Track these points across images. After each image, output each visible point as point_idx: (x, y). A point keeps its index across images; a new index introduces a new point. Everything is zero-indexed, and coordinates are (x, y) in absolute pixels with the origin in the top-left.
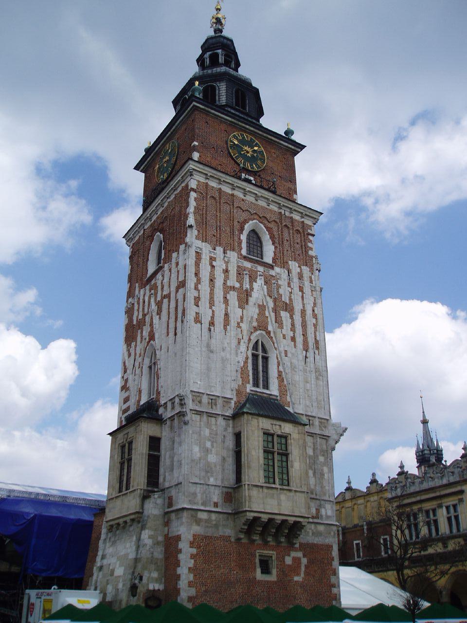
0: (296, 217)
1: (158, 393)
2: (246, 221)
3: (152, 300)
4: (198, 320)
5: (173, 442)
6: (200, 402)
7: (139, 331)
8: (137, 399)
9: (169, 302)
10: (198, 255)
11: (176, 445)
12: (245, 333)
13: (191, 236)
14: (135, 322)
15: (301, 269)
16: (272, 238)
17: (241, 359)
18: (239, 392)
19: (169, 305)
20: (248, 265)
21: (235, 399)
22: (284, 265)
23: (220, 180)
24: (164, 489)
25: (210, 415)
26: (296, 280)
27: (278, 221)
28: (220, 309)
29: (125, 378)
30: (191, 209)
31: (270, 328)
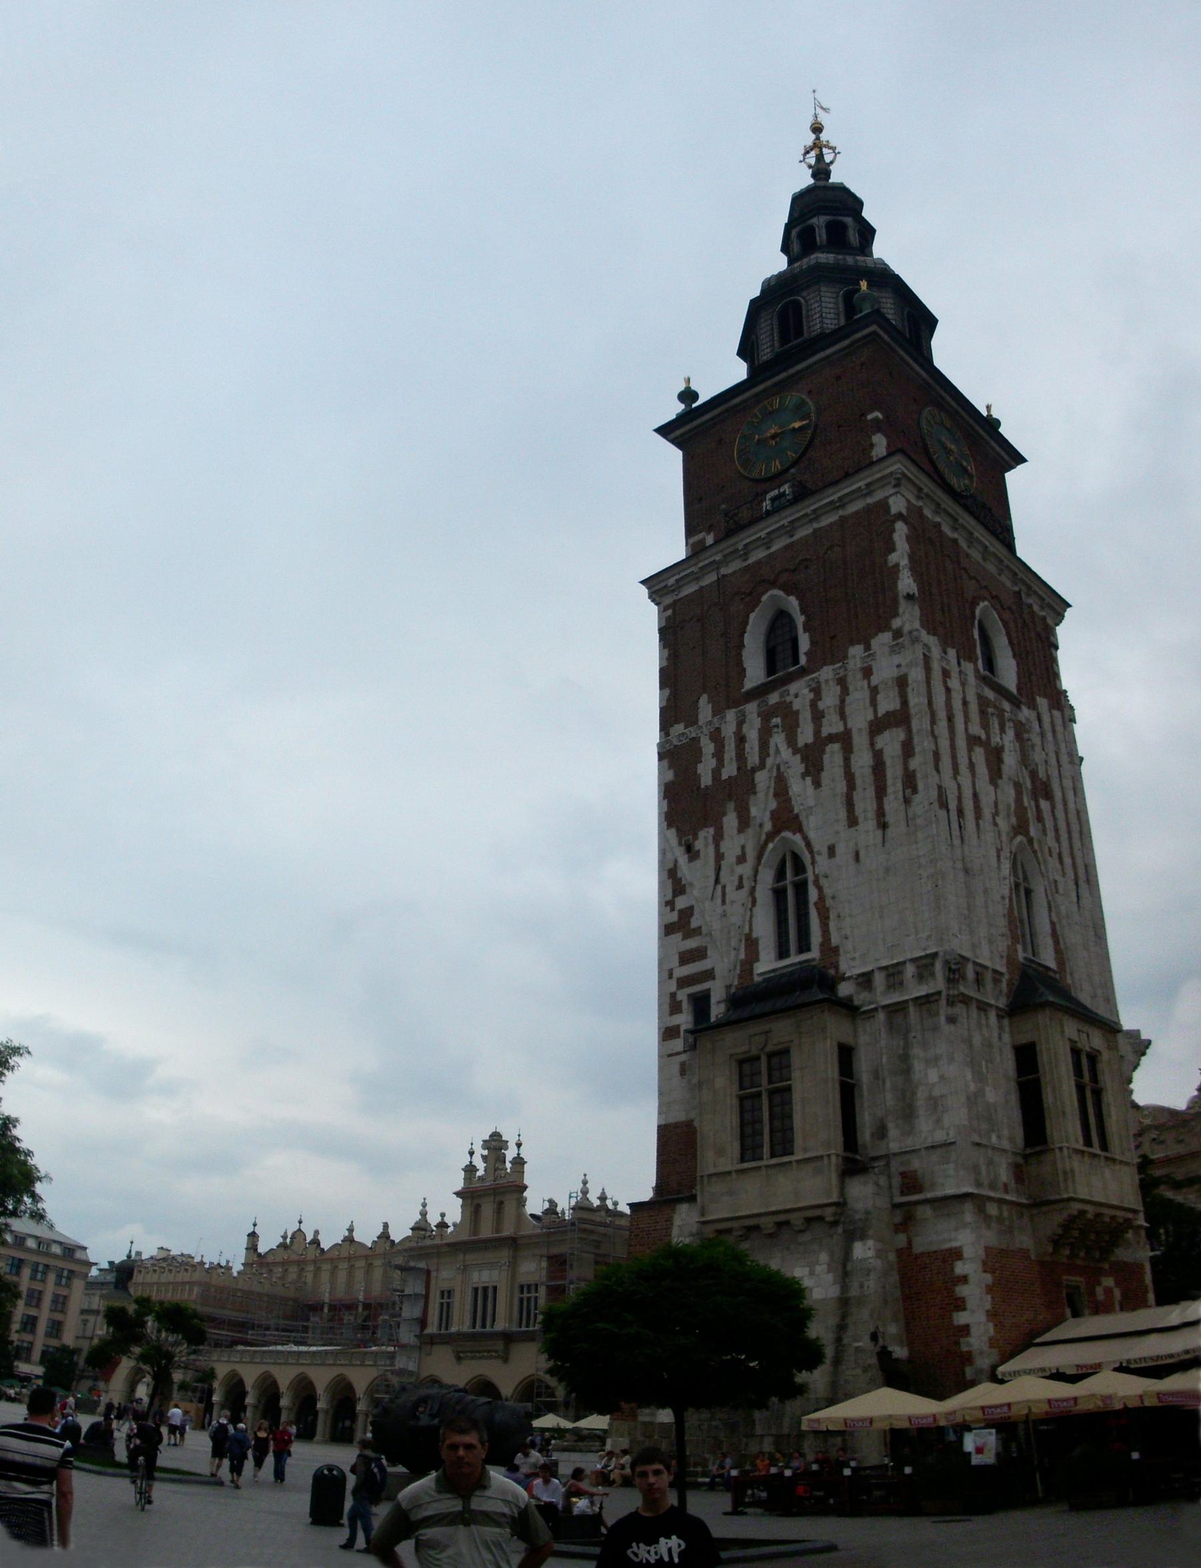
0: (1036, 608)
1: (830, 951)
2: (974, 604)
3: (778, 739)
4: (944, 805)
5: (905, 1058)
6: (963, 977)
7: (731, 806)
8: (742, 956)
9: (848, 750)
10: (927, 659)
11: (918, 1066)
12: (1004, 838)
13: (908, 618)
14: (706, 780)
15: (1052, 716)
16: (1011, 642)
17: (1006, 892)
18: (1011, 961)
19: (847, 760)
20: (989, 694)
21: (1007, 977)
22: (1033, 706)
23: (938, 505)
24: (886, 1156)
25: (983, 1007)
26: (1049, 736)
27: (1014, 608)
28: (965, 779)
29: (681, 902)
30: (900, 556)
31: (1033, 832)
